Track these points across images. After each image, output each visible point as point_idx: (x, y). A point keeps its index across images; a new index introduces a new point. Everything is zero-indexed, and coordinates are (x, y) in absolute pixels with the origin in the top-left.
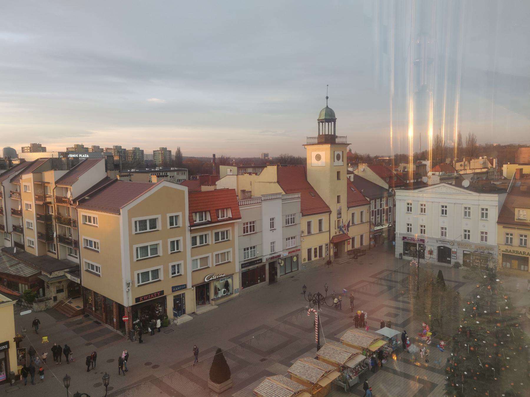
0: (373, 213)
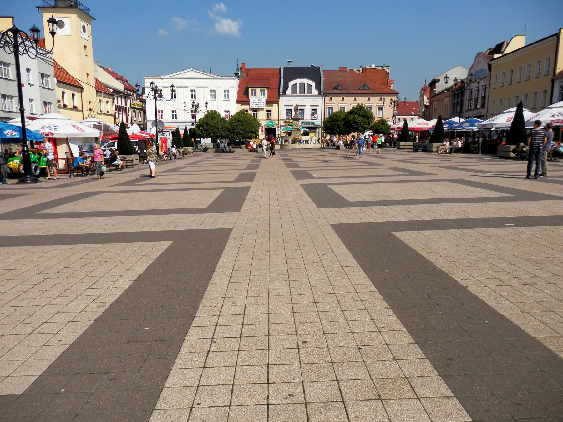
0: (116, 108)
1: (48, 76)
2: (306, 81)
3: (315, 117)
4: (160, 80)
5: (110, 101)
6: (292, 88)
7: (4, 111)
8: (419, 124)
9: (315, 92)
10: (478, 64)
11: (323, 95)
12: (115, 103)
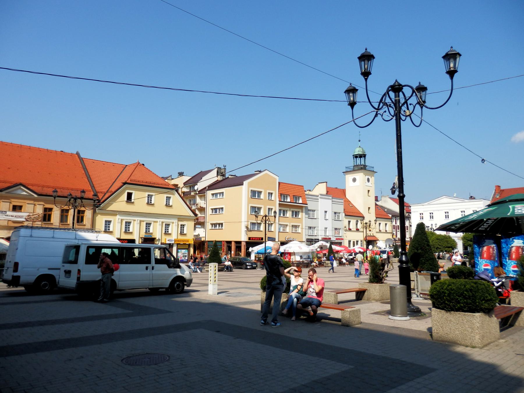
1: (339, 213)
4: (422, 206)
5: (389, 223)
7: (309, 236)
12: (394, 223)
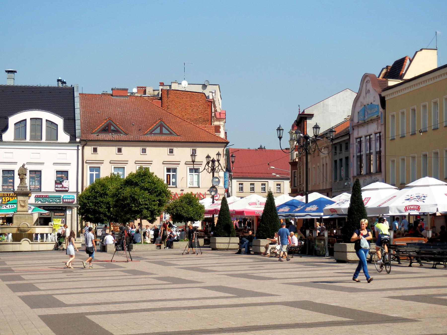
2: (45, 116)
3: (63, 187)
6: (16, 129)
8: (250, 204)
9: (64, 137)
10: (366, 94)
11: (80, 142)
